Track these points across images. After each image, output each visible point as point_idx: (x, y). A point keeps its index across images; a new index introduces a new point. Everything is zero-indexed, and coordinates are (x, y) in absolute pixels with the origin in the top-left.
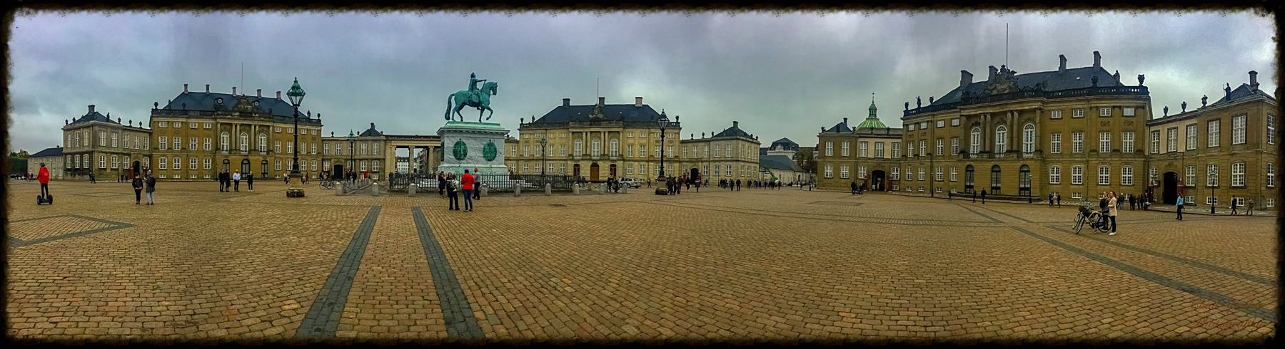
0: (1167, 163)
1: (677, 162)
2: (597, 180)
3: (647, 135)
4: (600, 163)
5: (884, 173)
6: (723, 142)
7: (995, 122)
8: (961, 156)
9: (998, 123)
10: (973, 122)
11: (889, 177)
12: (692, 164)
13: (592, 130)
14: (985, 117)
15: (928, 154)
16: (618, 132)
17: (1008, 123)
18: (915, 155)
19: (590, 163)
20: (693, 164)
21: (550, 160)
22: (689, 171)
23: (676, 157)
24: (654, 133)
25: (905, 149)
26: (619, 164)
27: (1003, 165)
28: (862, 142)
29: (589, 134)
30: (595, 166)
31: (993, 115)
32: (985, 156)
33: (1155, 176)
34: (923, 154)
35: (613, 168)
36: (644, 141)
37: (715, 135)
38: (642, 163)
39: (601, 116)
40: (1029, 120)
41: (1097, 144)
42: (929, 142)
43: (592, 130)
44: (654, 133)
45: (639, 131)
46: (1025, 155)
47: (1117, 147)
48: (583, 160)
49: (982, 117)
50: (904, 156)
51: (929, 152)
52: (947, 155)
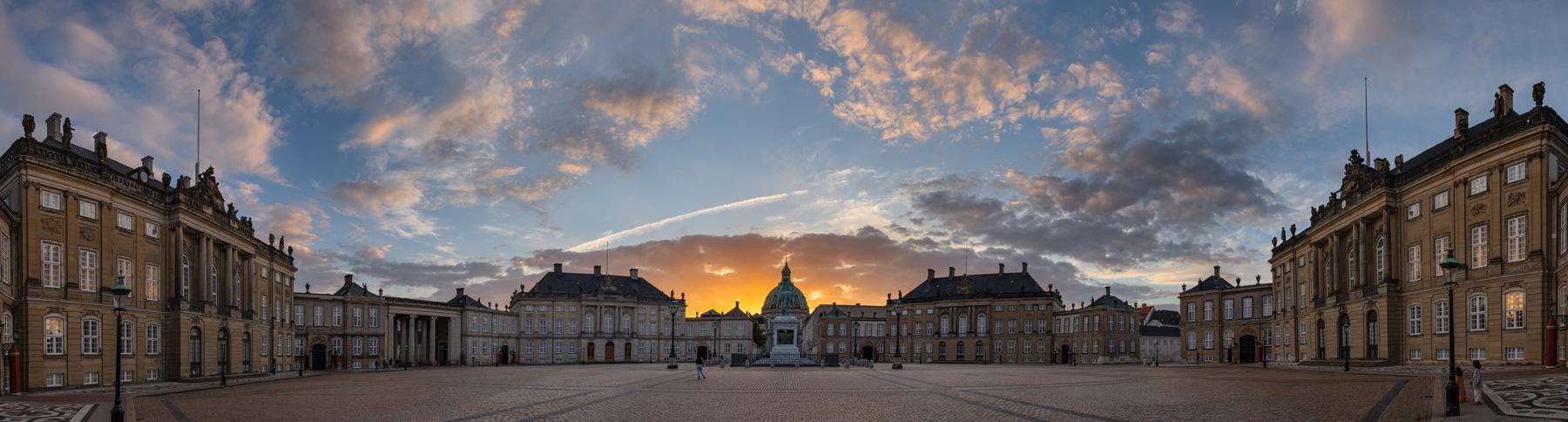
0: (1063, 339)
1: (683, 340)
2: (611, 360)
4: (616, 342)
6: (734, 322)
8: (936, 336)
13: (608, 304)
16: (632, 308)
19: (606, 341)
21: (557, 338)
23: (683, 335)
25: (889, 329)
26: (635, 342)
30: (610, 345)
33: (1058, 346)
35: (628, 347)
36: (654, 318)
38: (653, 341)
39: (613, 288)
40: (981, 312)
41: (1024, 327)
43: (608, 304)
45: (650, 307)
47: (1035, 329)
50: (888, 335)
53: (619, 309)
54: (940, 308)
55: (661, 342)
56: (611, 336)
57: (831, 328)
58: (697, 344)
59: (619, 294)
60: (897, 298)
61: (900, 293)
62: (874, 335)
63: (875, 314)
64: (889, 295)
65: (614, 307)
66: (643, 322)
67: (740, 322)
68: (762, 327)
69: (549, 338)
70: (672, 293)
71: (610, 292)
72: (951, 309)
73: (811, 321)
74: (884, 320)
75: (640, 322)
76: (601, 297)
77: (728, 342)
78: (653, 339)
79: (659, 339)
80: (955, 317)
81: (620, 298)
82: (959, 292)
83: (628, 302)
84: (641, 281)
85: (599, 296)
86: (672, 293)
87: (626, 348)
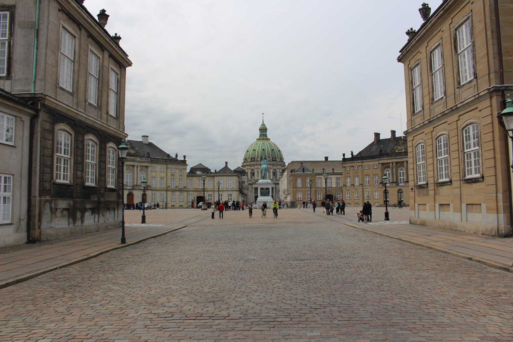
3: (165, 170)
4: (135, 192)
5: (332, 196)
6: (225, 177)
7: (398, 166)
9: (400, 167)
10: (386, 166)
11: (335, 198)
12: (198, 193)
14: (393, 164)
15: (360, 184)
16: (147, 167)
17: (405, 167)
18: (352, 185)
22: (196, 198)
23: (185, 187)
24: (170, 168)
26: (149, 193)
27: (403, 189)
28: (318, 178)
31: (397, 163)
32: (394, 185)
34: (357, 184)
36: (163, 175)
37: (217, 171)
38: (162, 192)
42: (361, 177)
44: (170, 168)
46: (400, 184)
49: (391, 164)
51: (361, 183)
52: (371, 184)
53: (137, 167)
54: (383, 164)
55: (169, 193)
56: (130, 188)
57: (299, 181)
58: (196, 195)
60: (350, 156)
61: (352, 153)
62: (334, 185)
63: (333, 169)
64: (344, 155)
65: (133, 166)
66: (155, 177)
67: (228, 178)
68: (245, 178)
70: (177, 156)
72: (391, 164)
73: (286, 173)
74: (341, 174)
75: (152, 177)
78: (162, 190)
79: (167, 191)
80: (394, 170)
82: (397, 151)
83: (144, 162)
84: (151, 145)
86: (177, 156)
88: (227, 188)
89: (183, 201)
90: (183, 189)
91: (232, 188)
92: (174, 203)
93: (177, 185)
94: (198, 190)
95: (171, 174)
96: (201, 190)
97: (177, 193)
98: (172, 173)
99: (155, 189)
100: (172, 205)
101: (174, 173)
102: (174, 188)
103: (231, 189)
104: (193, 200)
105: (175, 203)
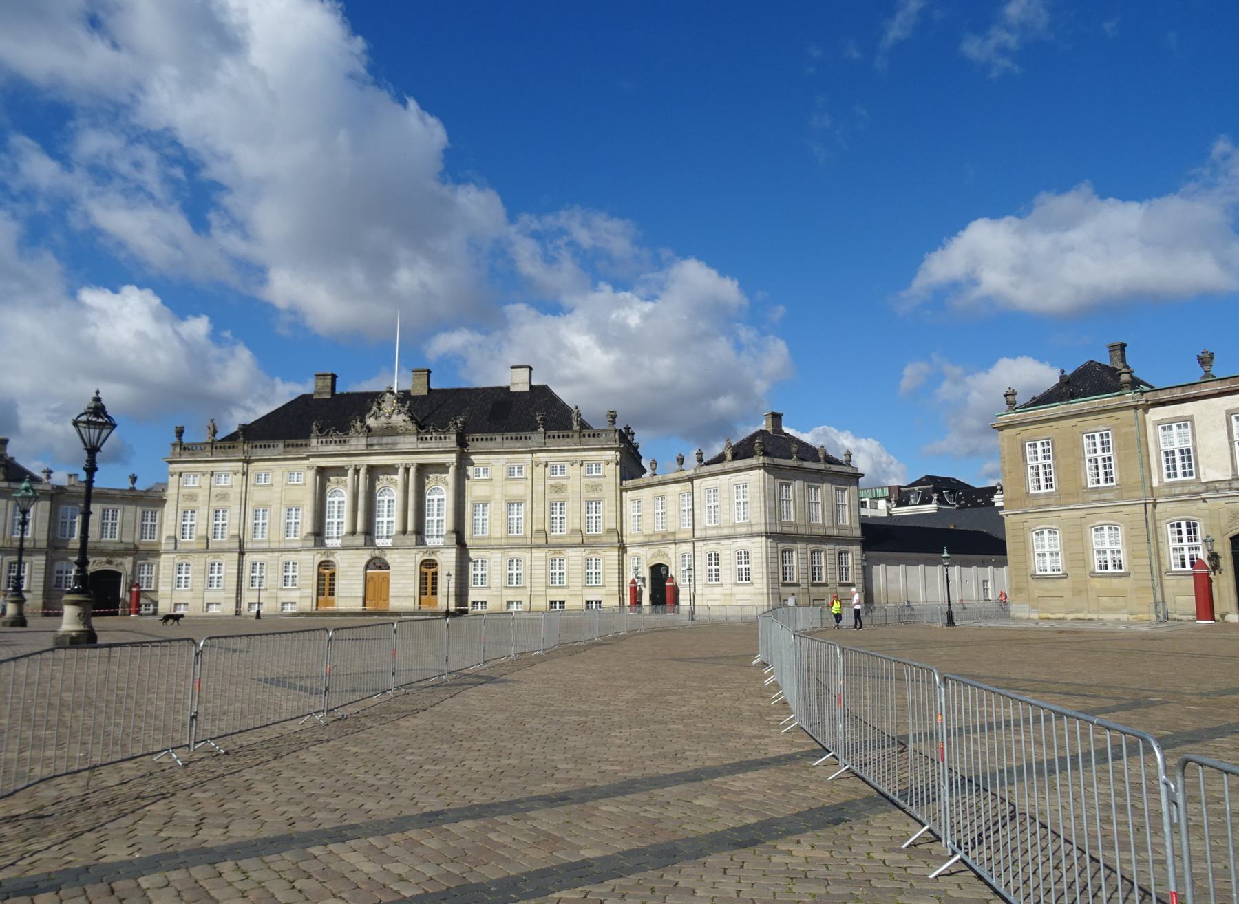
2: (381, 608)
3: (527, 471)
4: (391, 558)
16: (442, 468)
19: (365, 556)
20: (654, 550)
21: (253, 551)
22: (646, 573)
29: (362, 472)
36: (517, 490)
38: (514, 554)
48: (344, 548)
59: (406, 433)
69: (229, 551)
71: (390, 431)
76: (357, 442)
77: (712, 546)
78: (513, 547)
81: (410, 442)
85: (353, 441)
87: (423, 576)
88: (735, 526)
89: (604, 586)
90: (604, 540)
91: (750, 525)
92: (560, 591)
93: (577, 526)
94: (653, 539)
95: (552, 486)
96: (659, 538)
97: (571, 554)
98: (552, 482)
99: (485, 542)
100: (551, 602)
101: (564, 481)
102: (561, 537)
103: (743, 530)
104: (633, 582)
105: (565, 591)
